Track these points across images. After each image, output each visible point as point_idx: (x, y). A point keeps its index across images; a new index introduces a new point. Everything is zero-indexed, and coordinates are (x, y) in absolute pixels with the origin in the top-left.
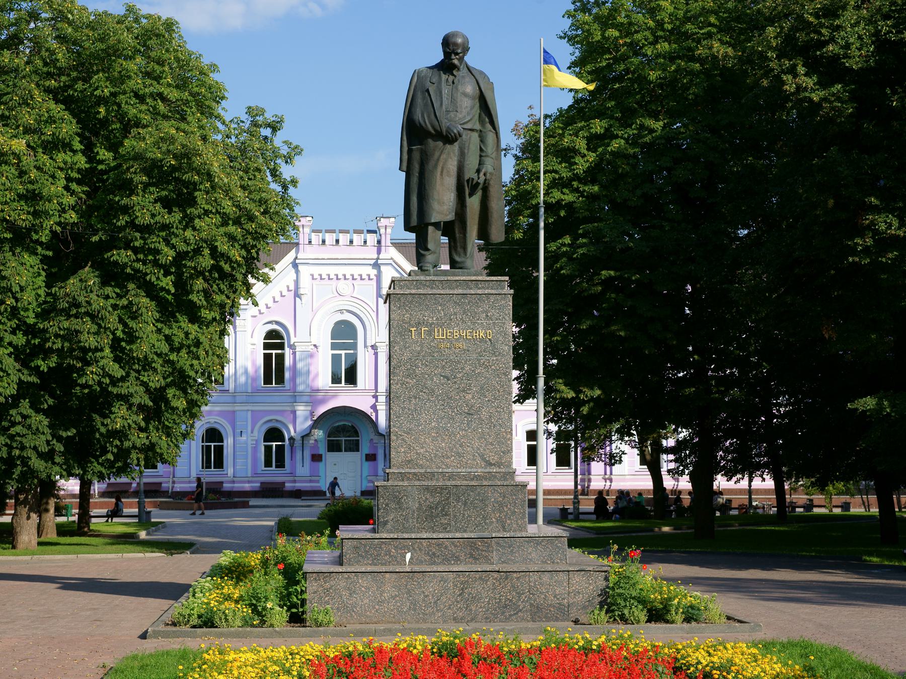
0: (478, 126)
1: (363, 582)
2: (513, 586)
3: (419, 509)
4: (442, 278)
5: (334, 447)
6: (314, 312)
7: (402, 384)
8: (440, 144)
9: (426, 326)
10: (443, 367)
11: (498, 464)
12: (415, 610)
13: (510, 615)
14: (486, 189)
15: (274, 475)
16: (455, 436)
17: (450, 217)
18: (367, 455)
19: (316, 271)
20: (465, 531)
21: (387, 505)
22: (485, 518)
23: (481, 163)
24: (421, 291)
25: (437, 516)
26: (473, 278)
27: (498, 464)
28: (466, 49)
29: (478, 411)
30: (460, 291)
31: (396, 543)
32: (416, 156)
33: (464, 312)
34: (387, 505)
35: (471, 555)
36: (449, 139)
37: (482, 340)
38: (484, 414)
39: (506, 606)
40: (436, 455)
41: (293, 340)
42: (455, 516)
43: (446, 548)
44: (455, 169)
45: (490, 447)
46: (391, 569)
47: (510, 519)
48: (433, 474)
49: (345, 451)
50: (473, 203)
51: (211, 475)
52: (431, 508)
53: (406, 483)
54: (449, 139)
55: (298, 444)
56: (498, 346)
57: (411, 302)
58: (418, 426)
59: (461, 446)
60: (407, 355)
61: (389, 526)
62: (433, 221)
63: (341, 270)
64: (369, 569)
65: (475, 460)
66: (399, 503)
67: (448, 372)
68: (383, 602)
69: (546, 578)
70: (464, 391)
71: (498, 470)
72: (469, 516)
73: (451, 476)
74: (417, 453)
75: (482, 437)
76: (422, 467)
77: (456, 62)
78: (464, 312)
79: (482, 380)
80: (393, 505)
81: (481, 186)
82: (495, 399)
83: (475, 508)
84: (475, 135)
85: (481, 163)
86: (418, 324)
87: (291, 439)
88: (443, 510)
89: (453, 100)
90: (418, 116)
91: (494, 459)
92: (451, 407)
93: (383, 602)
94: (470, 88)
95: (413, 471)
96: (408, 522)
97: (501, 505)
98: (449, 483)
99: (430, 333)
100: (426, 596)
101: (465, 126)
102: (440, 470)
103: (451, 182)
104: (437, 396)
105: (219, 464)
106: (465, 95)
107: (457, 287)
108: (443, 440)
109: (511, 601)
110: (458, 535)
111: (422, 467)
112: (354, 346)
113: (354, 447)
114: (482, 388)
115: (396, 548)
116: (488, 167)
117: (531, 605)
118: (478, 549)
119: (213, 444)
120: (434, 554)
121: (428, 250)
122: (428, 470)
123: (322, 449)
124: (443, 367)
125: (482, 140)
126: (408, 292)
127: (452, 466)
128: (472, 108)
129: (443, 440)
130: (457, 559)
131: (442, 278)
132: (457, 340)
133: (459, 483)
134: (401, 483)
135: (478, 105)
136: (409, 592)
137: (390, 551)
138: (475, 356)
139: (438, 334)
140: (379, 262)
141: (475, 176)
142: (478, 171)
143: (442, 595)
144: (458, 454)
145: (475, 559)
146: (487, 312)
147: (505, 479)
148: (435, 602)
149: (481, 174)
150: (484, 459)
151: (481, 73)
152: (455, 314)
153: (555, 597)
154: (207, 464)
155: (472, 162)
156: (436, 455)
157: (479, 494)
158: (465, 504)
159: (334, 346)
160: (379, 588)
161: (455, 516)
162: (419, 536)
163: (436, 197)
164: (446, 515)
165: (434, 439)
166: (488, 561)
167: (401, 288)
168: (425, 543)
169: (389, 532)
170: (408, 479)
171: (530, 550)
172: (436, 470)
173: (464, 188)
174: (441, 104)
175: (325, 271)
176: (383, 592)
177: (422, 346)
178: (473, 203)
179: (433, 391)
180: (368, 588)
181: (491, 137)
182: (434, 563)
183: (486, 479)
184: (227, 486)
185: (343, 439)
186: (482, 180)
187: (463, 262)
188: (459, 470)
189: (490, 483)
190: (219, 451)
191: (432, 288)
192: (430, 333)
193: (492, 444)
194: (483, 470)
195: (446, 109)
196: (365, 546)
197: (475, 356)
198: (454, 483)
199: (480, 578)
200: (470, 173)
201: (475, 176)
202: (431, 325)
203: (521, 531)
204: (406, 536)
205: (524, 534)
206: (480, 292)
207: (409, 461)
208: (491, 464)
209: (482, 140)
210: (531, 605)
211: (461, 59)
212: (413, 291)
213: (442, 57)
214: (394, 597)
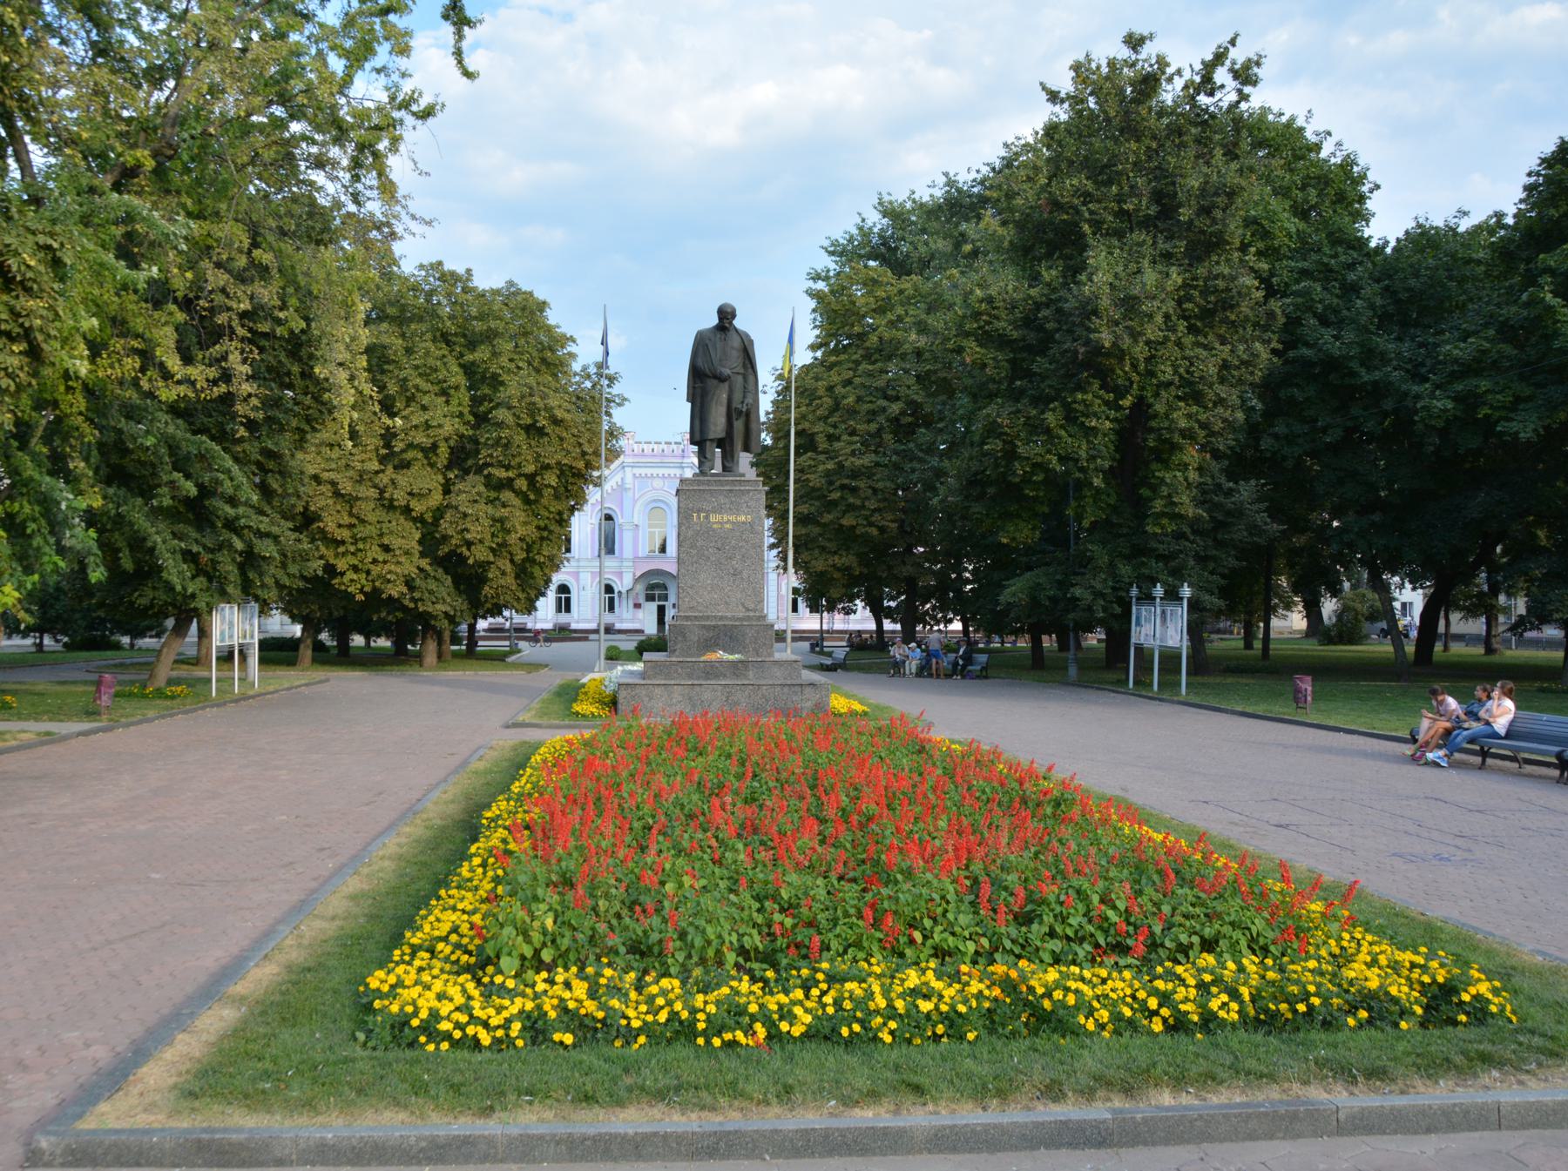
1: (658, 691)
6: (635, 501)
8: (715, 382)
14: (748, 414)
15: (608, 618)
17: (722, 435)
19: (637, 471)
28: (734, 316)
32: (699, 391)
36: (722, 379)
38: (745, 575)
50: (739, 425)
51: (563, 618)
54: (722, 379)
60: (690, 533)
73: (721, 618)
84: (740, 378)
86: (699, 511)
90: (700, 363)
91: (752, 606)
94: (736, 342)
99: (707, 517)
103: (722, 410)
105: (568, 610)
116: (749, 400)
123: (641, 600)
127: (722, 611)
139: (713, 519)
154: (559, 610)
155: (738, 396)
159: (650, 526)
166: (746, 677)
175: (643, 471)
178: (739, 425)
181: (751, 378)
184: (574, 626)
190: (568, 600)
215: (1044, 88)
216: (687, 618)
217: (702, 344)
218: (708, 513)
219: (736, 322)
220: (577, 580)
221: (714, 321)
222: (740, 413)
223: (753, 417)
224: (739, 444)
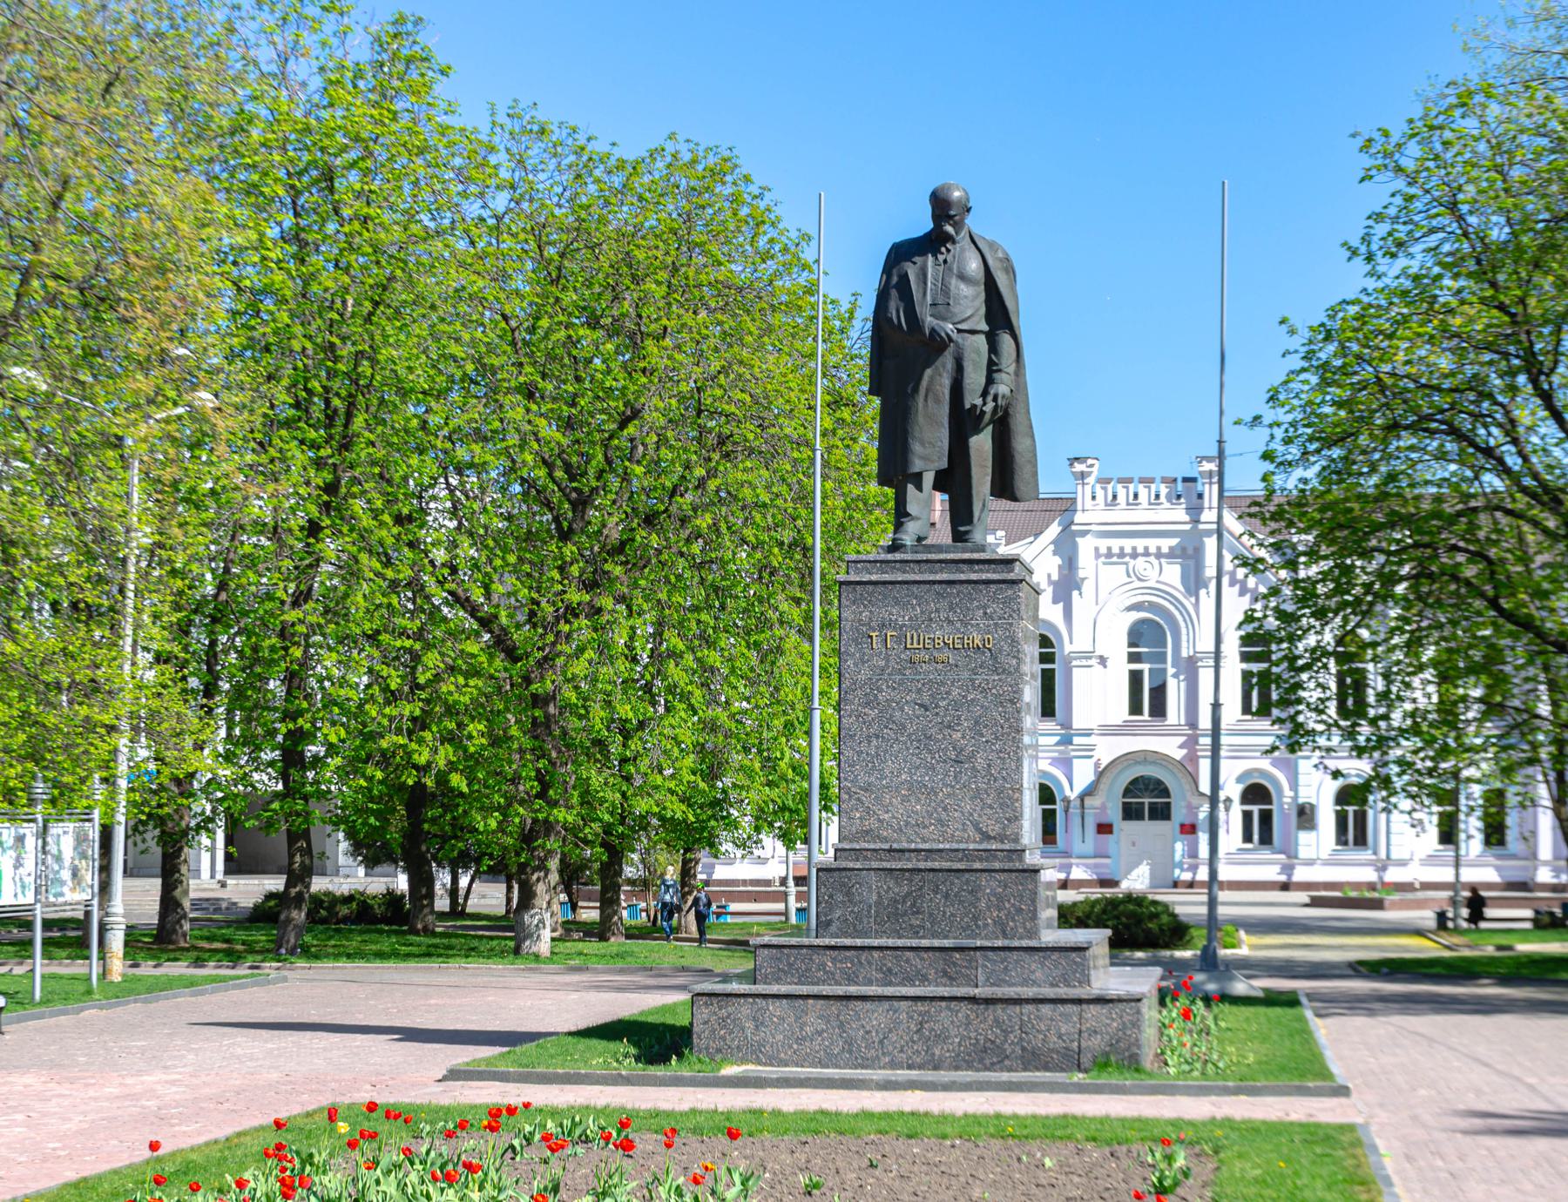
0: (985, 328)
1: (774, 1007)
2: (996, 1021)
3: (879, 903)
5: (1131, 813)
7: (858, 717)
9: (895, 629)
10: (919, 691)
11: (1001, 838)
12: (850, 1052)
13: (993, 1064)
16: (936, 794)
18: (1182, 826)
19: (1103, 544)
20: (946, 937)
21: (831, 896)
22: (975, 918)
23: (990, 381)
24: (886, 577)
25: (905, 914)
27: (1001, 838)
29: (972, 756)
30: (945, 576)
33: (951, 609)
34: (831, 896)
35: (945, 973)
38: (980, 762)
39: (985, 1050)
40: (907, 824)
41: (1068, 648)
42: (931, 915)
43: (907, 961)
44: (947, 392)
45: (989, 811)
46: (815, 990)
47: (1013, 920)
49: (1151, 818)
50: (981, 444)
52: (896, 901)
53: (858, 865)
55: (1075, 811)
56: (1002, 659)
57: (871, 594)
58: (881, 779)
59: (945, 809)
60: (864, 674)
61: (833, 928)
63: (1140, 544)
65: (964, 830)
66: (848, 894)
67: (926, 699)
68: (804, 1039)
69: (1046, 1009)
70: (949, 727)
71: (1000, 846)
72: (952, 915)
74: (880, 821)
75: (977, 795)
76: (886, 840)
77: (949, 229)
78: (951, 609)
79: (977, 710)
80: (839, 897)
81: (987, 417)
82: (997, 738)
83: (961, 902)
84: (981, 341)
85: (990, 381)
87: (1067, 801)
88: (913, 905)
89: (945, 290)
91: (993, 828)
92: (930, 752)
93: (804, 1039)
94: (974, 266)
95: (872, 846)
96: (861, 922)
97: (1000, 899)
98: (922, 865)
100: (868, 1032)
102: (913, 846)
104: (909, 735)
107: (941, 571)
108: (919, 800)
109: (993, 1042)
111: (886, 840)
112: (1162, 658)
113: (1161, 813)
114: (977, 723)
115: (834, 960)
116: (1002, 389)
117: (1023, 1049)
118: (955, 964)
120: (890, 970)
121: (908, 515)
122: (895, 846)
123: (1114, 814)
124: (919, 691)
125: (993, 348)
128: (975, 297)
129: (919, 800)
130: (924, 980)
133: (936, 865)
134: (851, 865)
135: (983, 295)
136: (841, 1025)
138: (966, 675)
140: (1201, 527)
141: (979, 402)
142: (985, 394)
143: (890, 1031)
144: (940, 821)
145: (951, 979)
146: (985, 607)
147: (1011, 860)
148: (881, 1042)
149: (990, 398)
150: (979, 830)
151: (993, 246)
152: (937, 611)
153: (1060, 1037)
155: (975, 378)
156: (907, 824)
157: (968, 880)
158: (947, 896)
159: (1134, 658)
160: (798, 1018)
161: (931, 915)
163: (917, 434)
164: (918, 912)
165: (905, 799)
167: (858, 571)
168: (876, 954)
169: (832, 936)
170: (866, 858)
171: (1034, 966)
172: (905, 845)
173: (963, 422)
174: (925, 294)
175: (1116, 544)
176: (805, 1024)
177: (887, 658)
178: (981, 444)
179: (904, 727)
180: (782, 1019)
181: (1006, 340)
182: (890, 984)
183: (981, 860)
185: (1146, 801)
187: (967, 532)
188: (941, 846)
189: (984, 865)
191: (904, 572)
193: (991, 807)
194: (977, 846)
195: (934, 299)
196: (788, 956)
197: (966, 675)
198: (929, 865)
199: (949, 1008)
200: (972, 399)
201: (979, 402)
202: (901, 627)
203: (1030, 938)
204: (848, 942)
206: (974, 577)
207: (867, 832)
208: (987, 837)
209: (993, 348)
210: (1023, 1049)
211: (958, 226)
212: (874, 578)
213: (930, 225)
214: (820, 1033)
219: (971, 222)
223: (1017, 423)
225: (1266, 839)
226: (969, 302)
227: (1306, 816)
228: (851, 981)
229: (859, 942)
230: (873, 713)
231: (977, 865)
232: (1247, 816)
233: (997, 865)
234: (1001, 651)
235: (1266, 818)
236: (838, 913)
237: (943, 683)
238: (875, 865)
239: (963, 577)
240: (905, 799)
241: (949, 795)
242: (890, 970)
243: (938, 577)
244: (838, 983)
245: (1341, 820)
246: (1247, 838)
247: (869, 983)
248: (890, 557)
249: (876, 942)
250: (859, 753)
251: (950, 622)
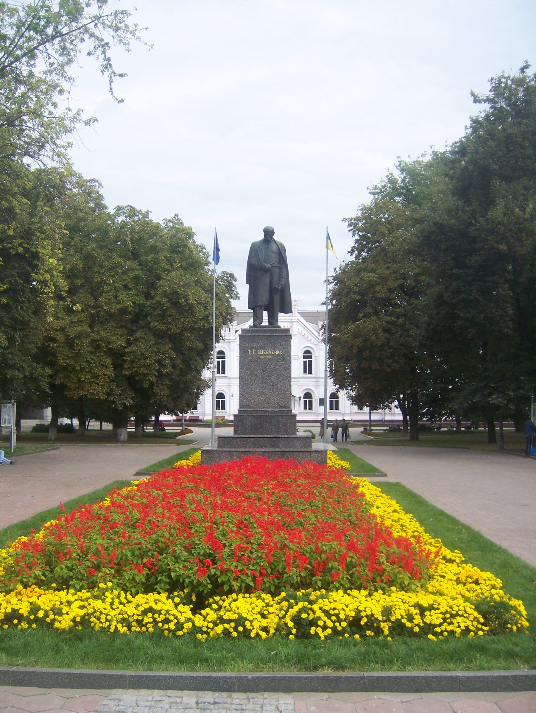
2: (287, 457)
4: (262, 329)
10: (262, 366)
17: (267, 303)
22: (278, 429)
23: (280, 280)
24: (253, 334)
26: (275, 329)
28: (273, 233)
29: (277, 384)
30: (269, 334)
31: (240, 439)
37: (278, 355)
38: (279, 386)
46: (236, 449)
48: (257, 411)
60: (247, 361)
61: (239, 432)
62: (259, 305)
64: (227, 450)
69: (301, 454)
73: (265, 412)
75: (278, 395)
76: (252, 408)
77: (269, 239)
80: (240, 424)
84: (277, 270)
86: (251, 349)
91: (283, 404)
98: (263, 415)
99: (256, 352)
101: (273, 265)
103: (267, 288)
105: (224, 408)
106: (273, 252)
107: (268, 333)
110: (266, 436)
111: (252, 408)
114: (278, 375)
119: (221, 400)
124: (262, 366)
126: (247, 335)
129: (262, 397)
130: (265, 446)
131: (262, 329)
132: (268, 355)
133: (268, 415)
137: (237, 442)
138: (275, 361)
139: (260, 352)
141: (277, 286)
146: (280, 343)
154: (218, 408)
155: (276, 279)
162: (249, 436)
165: (258, 396)
166: (278, 447)
173: (272, 290)
177: (253, 357)
178: (277, 298)
181: (285, 270)
182: (256, 448)
186: (279, 288)
189: (281, 415)
192: (256, 352)
198: (265, 414)
199: (273, 454)
204: (244, 436)
205: (293, 436)
206: (277, 334)
208: (281, 407)
211: (272, 238)
212: (249, 334)
213: (263, 237)
215: (473, 94)
216: (245, 412)
217: (254, 250)
218: (257, 349)
220: (229, 390)
221: (261, 237)
222: (277, 289)
224: (277, 305)
225: (311, 408)
226: (274, 259)
227: (322, 402)
228: (245, 447)
229: (247, 436)
230: (249, 372)
231: (279, 415)
232: (305, 402)
233: (284, 414)
234: (285, 355)
235: (311, 402)
236: (240, 428)
237: (269, 364)
238: (250, 415)
239: (274, 335)
240: (258, 396)
241: (270, 395)
242: (256, 444)
243: (267, 335)
244: (241, 448)
245: (331, 402)
246: (305, 408)
247: (250, 447)
248: (253, 329)
249: (252, 436)
250: (245, 384)
251: (271, 347)
